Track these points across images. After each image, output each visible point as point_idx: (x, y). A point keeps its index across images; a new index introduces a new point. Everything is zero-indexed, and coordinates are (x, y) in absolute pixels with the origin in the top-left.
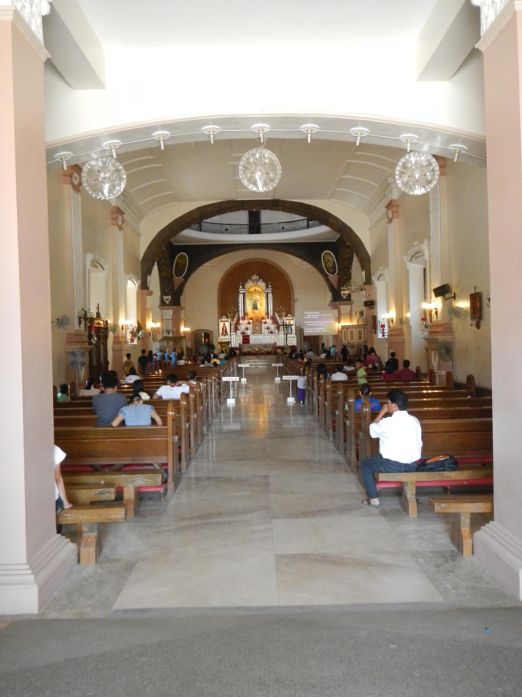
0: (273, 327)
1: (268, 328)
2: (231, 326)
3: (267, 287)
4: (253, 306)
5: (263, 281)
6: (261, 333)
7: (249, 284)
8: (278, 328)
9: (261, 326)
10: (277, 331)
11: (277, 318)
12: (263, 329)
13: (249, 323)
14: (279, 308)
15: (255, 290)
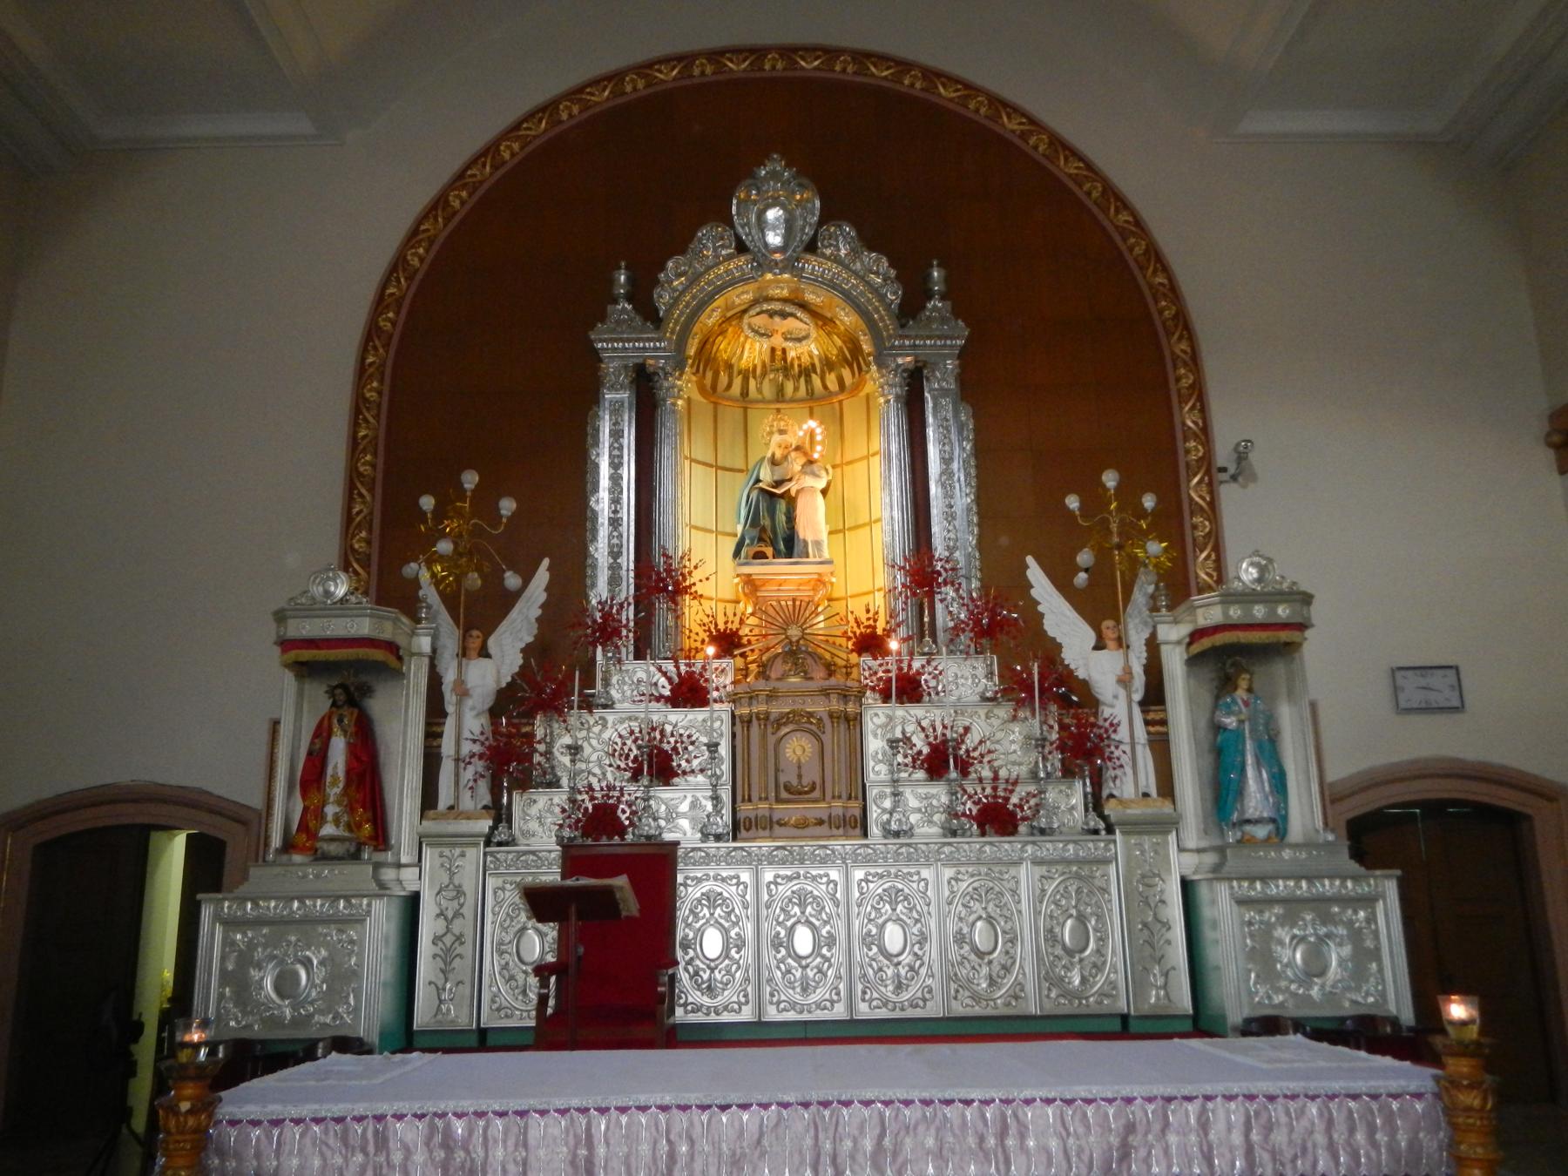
0: (1009, 743)
1: (940, 760)
2: (432, 735)
3: (909, 310)
4: (754, 520)
5: (870, 240)
6: (861, 825)
7: (701, 274)
8: (1082, 750)
9: (853, 722)
10: (1070, 799)
12: (877, 771)
13: (689, 692)
14: (1094, 498)
15: (779, 363)
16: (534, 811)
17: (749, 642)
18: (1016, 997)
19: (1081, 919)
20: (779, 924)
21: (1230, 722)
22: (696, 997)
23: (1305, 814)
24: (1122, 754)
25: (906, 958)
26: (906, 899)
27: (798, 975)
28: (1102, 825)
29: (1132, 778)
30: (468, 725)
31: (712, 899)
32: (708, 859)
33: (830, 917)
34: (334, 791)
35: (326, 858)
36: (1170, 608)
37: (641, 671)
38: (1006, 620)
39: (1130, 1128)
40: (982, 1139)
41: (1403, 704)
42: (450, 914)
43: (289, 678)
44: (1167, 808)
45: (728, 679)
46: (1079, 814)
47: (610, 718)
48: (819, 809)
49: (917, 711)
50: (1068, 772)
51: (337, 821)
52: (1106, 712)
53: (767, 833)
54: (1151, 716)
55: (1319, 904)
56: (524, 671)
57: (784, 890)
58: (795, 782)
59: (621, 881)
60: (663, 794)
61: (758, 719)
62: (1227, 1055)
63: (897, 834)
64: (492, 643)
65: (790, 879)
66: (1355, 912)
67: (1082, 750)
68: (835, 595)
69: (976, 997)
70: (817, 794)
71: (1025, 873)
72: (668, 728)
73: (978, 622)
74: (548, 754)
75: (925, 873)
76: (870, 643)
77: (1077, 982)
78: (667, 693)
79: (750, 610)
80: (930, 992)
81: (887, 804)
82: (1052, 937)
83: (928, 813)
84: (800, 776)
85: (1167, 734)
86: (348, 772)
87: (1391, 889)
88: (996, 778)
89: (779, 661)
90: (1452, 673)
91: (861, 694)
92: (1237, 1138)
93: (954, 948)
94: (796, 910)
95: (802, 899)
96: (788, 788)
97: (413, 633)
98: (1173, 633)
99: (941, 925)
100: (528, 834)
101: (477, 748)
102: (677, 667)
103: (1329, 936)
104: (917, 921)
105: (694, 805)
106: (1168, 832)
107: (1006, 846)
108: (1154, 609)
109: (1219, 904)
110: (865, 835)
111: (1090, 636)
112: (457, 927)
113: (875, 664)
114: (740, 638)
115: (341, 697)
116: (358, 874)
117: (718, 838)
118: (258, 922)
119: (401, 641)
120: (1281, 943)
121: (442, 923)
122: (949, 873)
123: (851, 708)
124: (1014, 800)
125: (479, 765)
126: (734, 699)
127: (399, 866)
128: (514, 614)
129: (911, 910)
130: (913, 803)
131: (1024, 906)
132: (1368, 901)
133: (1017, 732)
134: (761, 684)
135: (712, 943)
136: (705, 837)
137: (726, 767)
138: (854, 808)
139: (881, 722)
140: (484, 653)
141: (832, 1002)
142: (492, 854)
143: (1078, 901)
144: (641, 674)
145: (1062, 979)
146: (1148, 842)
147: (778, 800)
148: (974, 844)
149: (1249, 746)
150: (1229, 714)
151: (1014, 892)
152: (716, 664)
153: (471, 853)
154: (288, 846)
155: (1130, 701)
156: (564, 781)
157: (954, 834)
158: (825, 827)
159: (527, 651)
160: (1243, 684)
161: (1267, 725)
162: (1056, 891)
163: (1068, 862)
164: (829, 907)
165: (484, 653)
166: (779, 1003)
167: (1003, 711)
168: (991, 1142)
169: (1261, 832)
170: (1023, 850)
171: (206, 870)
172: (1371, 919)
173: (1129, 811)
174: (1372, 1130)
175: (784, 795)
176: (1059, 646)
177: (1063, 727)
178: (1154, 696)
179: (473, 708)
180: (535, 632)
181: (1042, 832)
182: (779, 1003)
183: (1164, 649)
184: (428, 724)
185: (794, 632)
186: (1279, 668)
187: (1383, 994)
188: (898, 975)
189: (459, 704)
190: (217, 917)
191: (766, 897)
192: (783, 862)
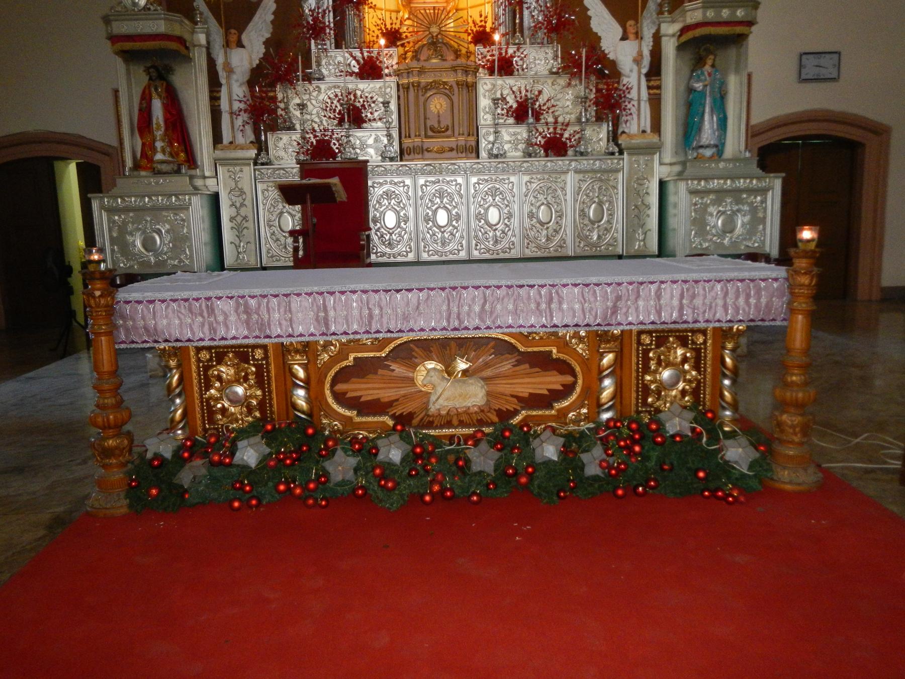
0: (565, 100)
1: (523, 112)
2: (214, 98)
8: (608, 104)
9: (471, 88)
10: (599, 136)
11: (604, 24)
12: (485, 118)
13: (370, 70)
16: (281, 144)
17: (406, 36)
18: (561, 247)
19: (600, 204)
20: (428, 208)
21: (699, 86)
22: (382, 248)
23: (735, 142)
24: (632, 107)
25: (500, 227)
26: (501, 193)
27: (439, 236)
28: (616, 150)
29: (636, 121)
30: (235, 92)
31: (388, 195)
32: (386, 172)
33: (457, 204)
34: (159, 134)
35: (160, 173)
36: (670, 12)
37: (340, 56)
38: (568, 20)
39: (618, 298)
40: (538, 304)
41: (804, 76)
42: (238, 205)
43: (119, 62)
44: (655, 139)
45: (395, 61)
46: (603, 144)
47: (323, 87)
48: (451, 142)
49: (510, 81)
50: (599, 119)
51: (163, 151)
52: (625, 80)
53: (420, 156)
54: (652, 83)
55: (736, 193)
56: (266, 57)
57: (431, 189)
58: (436, 125)
59: (335, 180)
60: (358, 133)
61: (413, 86)
62: (675, 264)
63: (496, 156)
64: (244, 38)
65: (434, 183)
66: (755, 197)
67: (608, 104)
68: (461, 6)
69: (539, 247)
70: (449, 132)
71: (570, 179)
72: (359, 93)
73: (550, 22)
74: (286, 109)
75: (512, 179)
76: (482, 37)
77: (595, 238)
78: (357, 70)
79: (406, 16)
80: (513, 244)
81: (491, 138)
82: (583, 214)
83: (515, 144)
84: (439, 122)
85: (660, 94)
86: (166, 121)
87: (778, 184)
88: (556, 122)
89: (425, 49)
90: (836, 56)
91: (476, 71)
92: (675, 302)
93: (527, 220)
94: (438, 200)
95: (441, 194)
96: (432, 129)
97: (193, 32)
98: (670, 29)
99: (521, 208)
100: (279, 158)
101: (242, 106)
102: (362, 53)
103: (739, 211)
104: (507, 206)
105: (377, 140)
106: (655, 153)
107: (560, 163)
108: (660, 13)
109: (680, 195)
110: (478, 157)
111: (619, 31)
112: (243, 211)
113: (484, 51)
114: (401, 34)
115: (154, 74)
116: (181, 182)
117: (392, 159)
118: (127, 210)
119: (187, 36)
120: (711, 215)
121: (234, 209)
122: (526, 178)
123: (470, 79)
124: (566, 135)
125: (244, 116)
126: (398, 73)
127: (204, 177)
128: (256, 18)
129: (503, 200)
130: (507, 138)
131: (568, 197)
132: (763, 191)
133: (570, 94)
134: (415, 64)
135: (390, 220)
136: (384, 158)
137: (395, 117)
138: (472, 141)
139: (488, 87)
140: (240, 45)
141: (459, 251)
142: (259, 170)
143: (599, 194)
144: (340, 59)
145: (587, 237)
146: (642, 159)
147: (427, 137)
148: (542, 162)
149: (708, 100)
150: (698, 81)
151: (563, 189)
152: (386, 51)
153: (246, 169)
154: (137, 167)
155: (639, 73)
156: (298, 126)
157: (530, 156)
158: (454, 152)
159: (267, 43)
160: (709, 62)
161: (720, 88)
162: (587, 188)
163: (594, 171)
164: (457, 198)
165: (240, 45)
166: (429, 251)
167: (562, 81)
168: (543, 306)
169: (708, 153)
170: (570, 165)
171: (91, 182)
172: (764, 201)
173: (633, 141)
174: (748, 296)
175: (430, 133)
176: (599, 38)
177: (598, 91)
178: (655, 71)
179: (237, 81)
180: (271, 30)
181: (582, 154)
182: (429, 251)
183: (664, 39)
184: (211, 91)
185: (434, 30)
186: (732, 52)
187: (763, 242)
188: (496, 236)
189: (228, 78)
190: (102, 207)
191: (420, 193)
192: (430, 173)
